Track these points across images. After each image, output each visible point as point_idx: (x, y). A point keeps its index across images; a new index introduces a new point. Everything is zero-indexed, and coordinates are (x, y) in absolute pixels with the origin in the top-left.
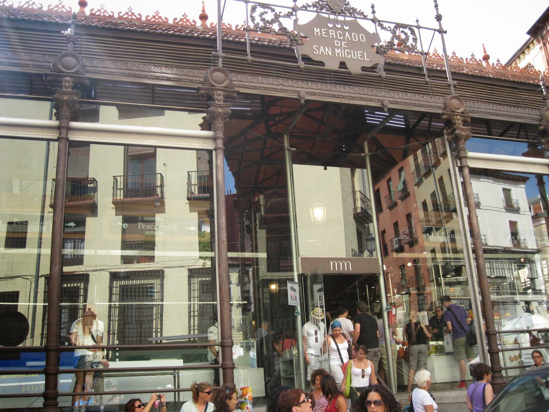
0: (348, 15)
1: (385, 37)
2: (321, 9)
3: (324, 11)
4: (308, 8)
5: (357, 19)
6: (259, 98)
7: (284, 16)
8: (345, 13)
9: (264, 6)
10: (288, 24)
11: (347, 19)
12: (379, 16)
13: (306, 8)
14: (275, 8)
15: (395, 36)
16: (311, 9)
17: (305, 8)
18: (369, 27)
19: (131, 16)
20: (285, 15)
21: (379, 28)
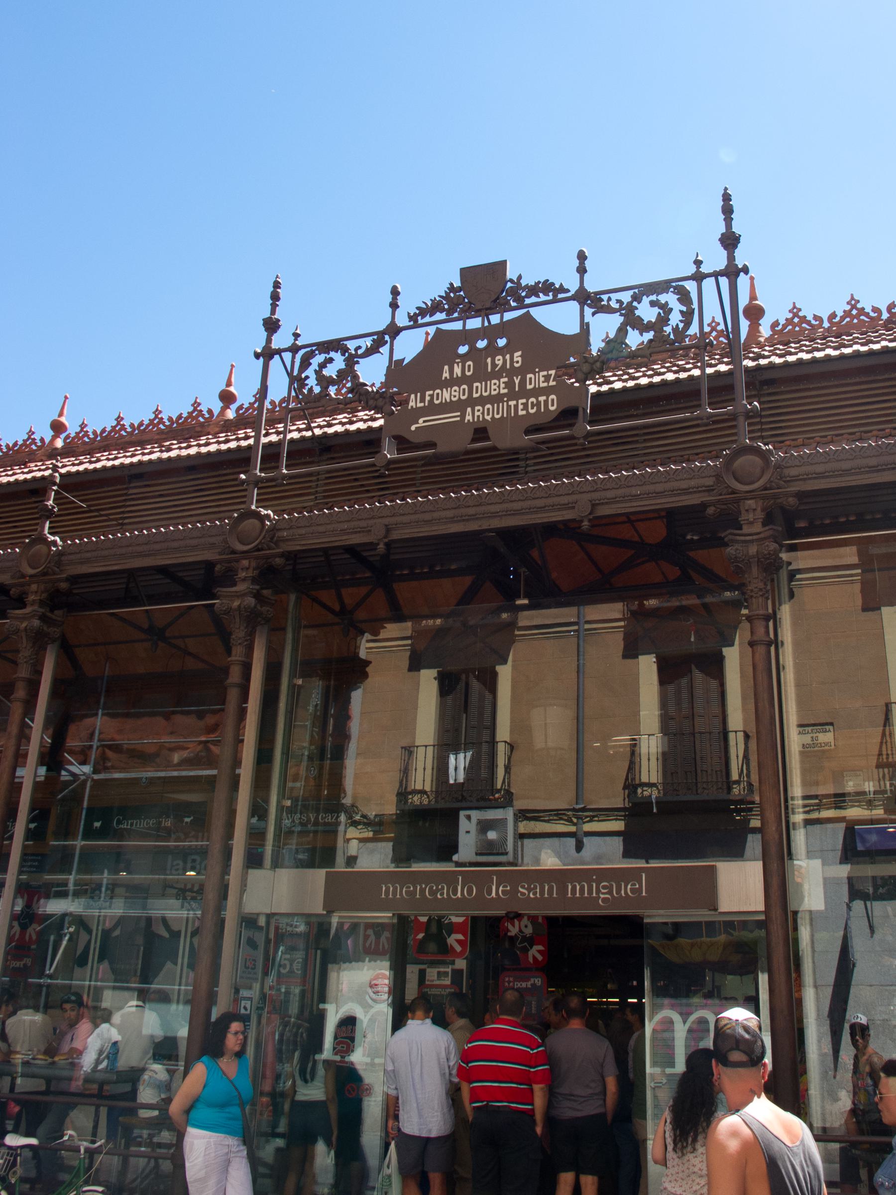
0: (513, 304)
1: (602, 328)
2: (450, 312)
3: (456, 315)
4: (420, 321)
5: (533, 311)
6: (321, 553)
7: (365, 355)
8: (508, 302)
9: (327, 346)
10: (372, 373)
11: (509, 316)
12: (591, 286)
13: (416, 321)
14: (345, 343)
15: (632, 320)
16: (427, 319)
17: (414, 321)
18: (560, 319)
19: (857, 317)
20: (367, 349)
21: (588, 311)
